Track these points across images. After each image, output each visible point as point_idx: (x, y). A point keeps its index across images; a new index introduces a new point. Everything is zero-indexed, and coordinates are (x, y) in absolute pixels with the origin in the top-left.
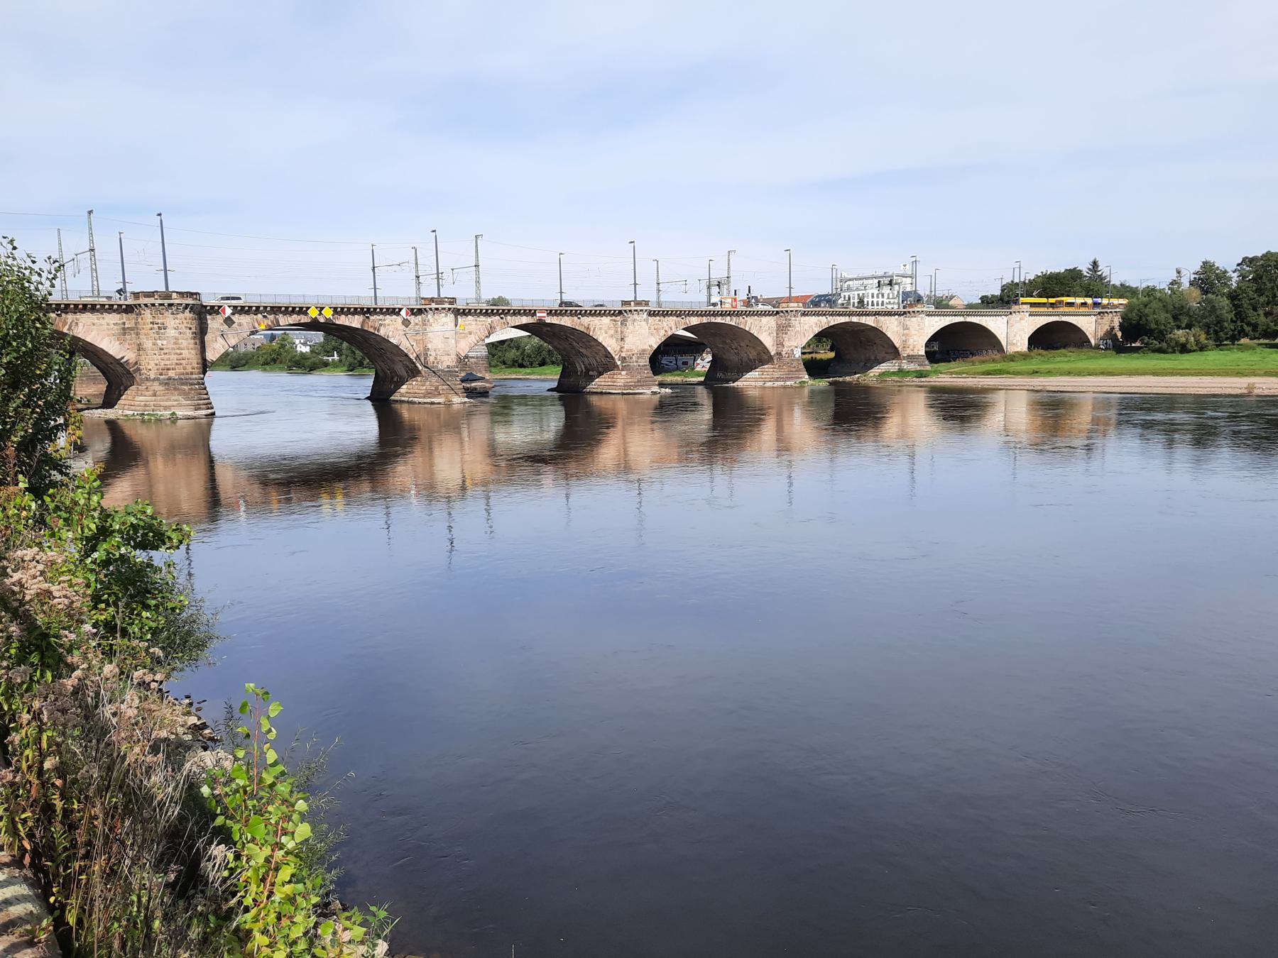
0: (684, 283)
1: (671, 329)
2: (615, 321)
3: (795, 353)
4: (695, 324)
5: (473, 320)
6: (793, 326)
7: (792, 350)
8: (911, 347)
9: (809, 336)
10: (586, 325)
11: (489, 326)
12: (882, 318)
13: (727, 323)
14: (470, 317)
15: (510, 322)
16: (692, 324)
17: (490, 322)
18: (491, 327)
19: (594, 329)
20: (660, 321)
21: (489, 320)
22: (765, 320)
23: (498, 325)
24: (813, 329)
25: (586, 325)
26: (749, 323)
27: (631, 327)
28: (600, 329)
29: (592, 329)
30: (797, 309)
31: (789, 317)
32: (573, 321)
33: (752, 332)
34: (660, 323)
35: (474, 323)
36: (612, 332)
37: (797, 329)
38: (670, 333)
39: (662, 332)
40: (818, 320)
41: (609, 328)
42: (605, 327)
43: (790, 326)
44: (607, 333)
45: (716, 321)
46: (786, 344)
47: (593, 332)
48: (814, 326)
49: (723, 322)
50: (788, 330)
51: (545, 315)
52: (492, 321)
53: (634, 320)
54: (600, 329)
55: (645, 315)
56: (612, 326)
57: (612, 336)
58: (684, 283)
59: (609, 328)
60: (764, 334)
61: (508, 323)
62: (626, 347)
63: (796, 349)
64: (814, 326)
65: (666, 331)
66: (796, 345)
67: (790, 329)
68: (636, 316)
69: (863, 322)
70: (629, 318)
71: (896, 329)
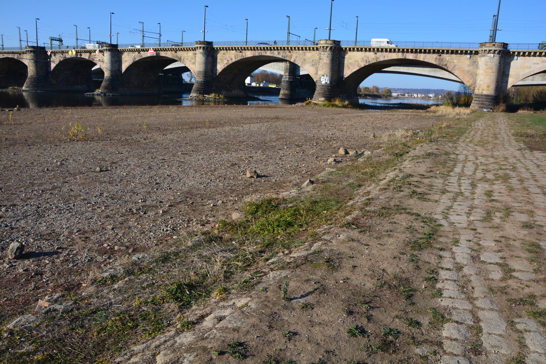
1: (232, 59)
3: (322, 80)
4: (249, 56)
8: (478, 87)
9: (353, 69)
10: (179, 57)
13: (275, 56)
16: (247, 57)
20: (224, 54)
21: (134, 55)
24: (359, 64)
25: (179, 57)
32: (172, 55)
34: (224, 56)
35: (127, 56)
38: (230, 62)
39: (225, 61)
40: (365, 56)
41: (192, 58)
42: (190, 59)
44: (190, 61)
45: (266, 55)
48: (360, 61)
49: (272, 55)
63: (323, 77)
64: (360, 61)
65: (228, 61)
69: (421, 60)
71: (467, 68)
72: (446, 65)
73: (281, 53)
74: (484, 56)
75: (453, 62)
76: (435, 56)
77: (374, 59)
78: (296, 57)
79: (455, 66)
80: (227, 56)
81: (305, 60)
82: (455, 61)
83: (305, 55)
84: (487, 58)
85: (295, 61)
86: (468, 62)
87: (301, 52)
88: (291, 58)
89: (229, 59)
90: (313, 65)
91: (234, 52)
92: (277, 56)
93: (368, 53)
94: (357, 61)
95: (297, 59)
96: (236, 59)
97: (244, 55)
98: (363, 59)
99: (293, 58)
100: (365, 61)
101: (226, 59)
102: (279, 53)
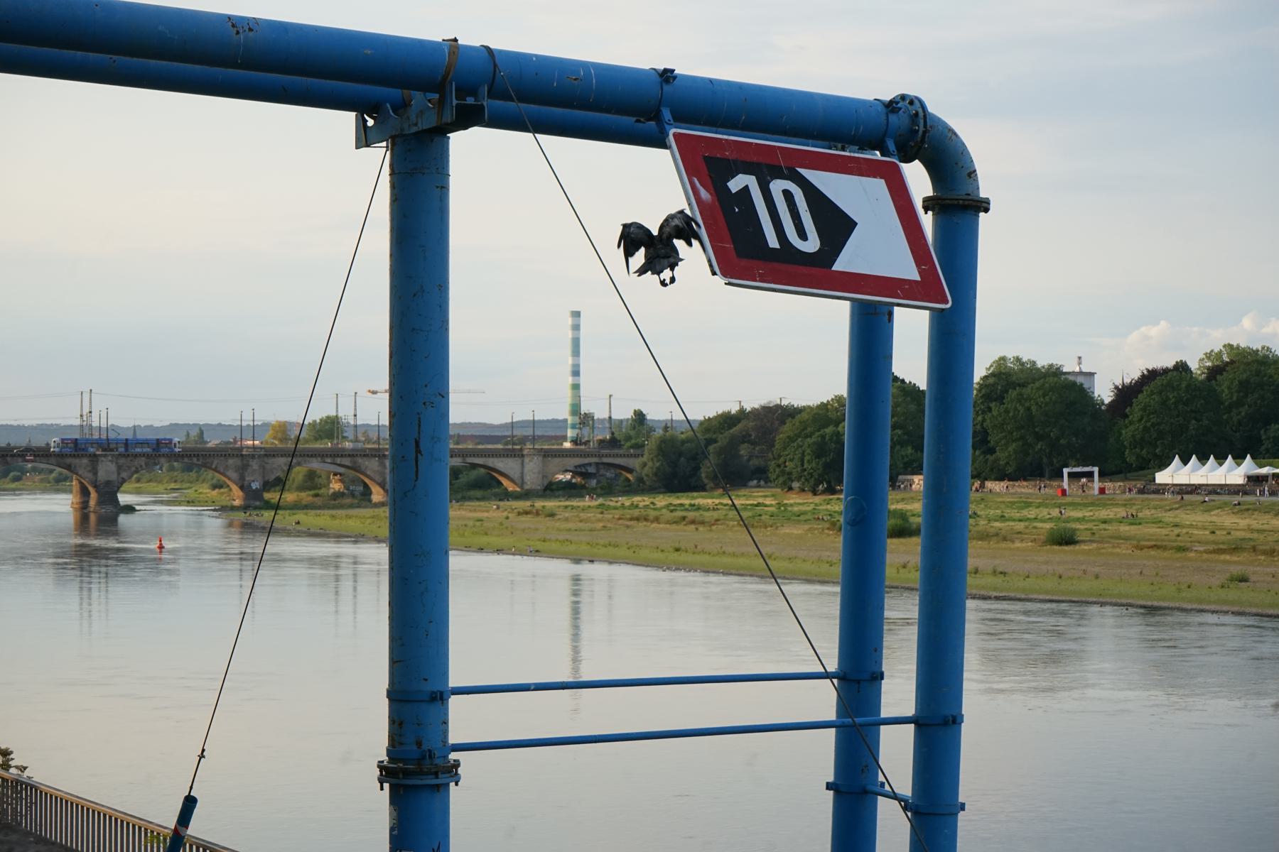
1: (141, 466)
7: (250, 484)
12: (360, 460)
20: (131, 461)
22: (231, 461)
36: (89, 468)
37: (254, 468)
39: (134, 469)
44: (85, 468)
46: (247, 479)
53: (102, 461)
55: (110, 458)
57: (90, 471)
60: (230, 471)
62: (99, 478)
66: (252, 479)
68: (103, 459)
71: (376, 469)
73: (201, 460)
76: (349, 459)
80: (136, 463)
81: (227, 466)
83: (227, 461)
86: (377, 463)
87: (222, 458)
90: (236, 471)
91: (143, 458)
94: (280, 466)
97: (156, 461)
101: (134, 466)
102: (198, 460)
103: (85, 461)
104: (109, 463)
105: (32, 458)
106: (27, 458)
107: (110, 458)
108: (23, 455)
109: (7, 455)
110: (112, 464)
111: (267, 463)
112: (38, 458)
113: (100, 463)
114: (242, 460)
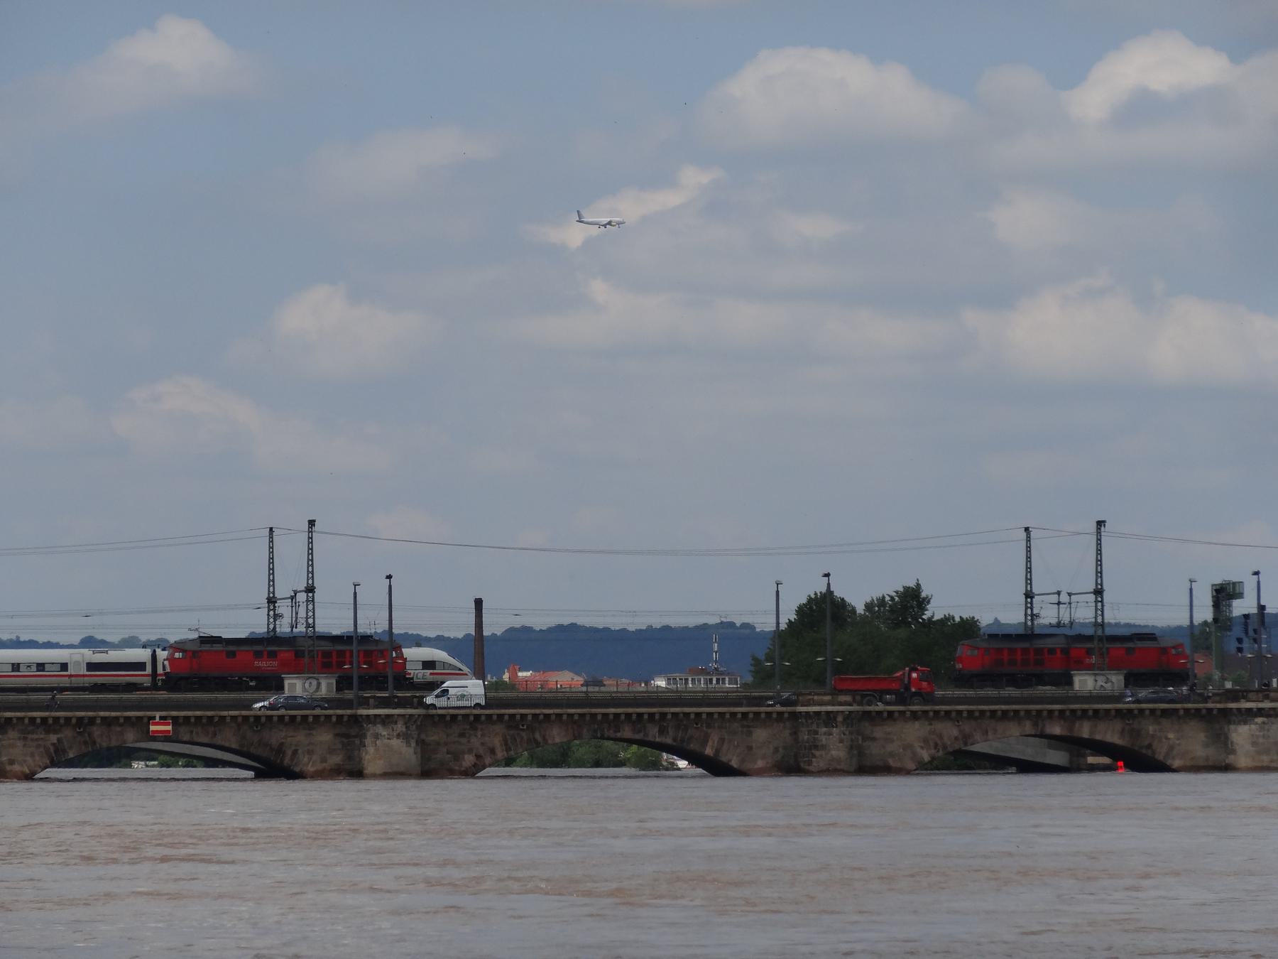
0: (1054, 598)
1: (493, 751)
2: (347, 736)
5: (19, 739)
6: (824, 747)
11: (52, 750)
14: (12, 734)
15: (98, 740)
17: (55, 741)
18: (56, 751)
19: (295, 752)
20: (462, 735)
21: (53, 738)
22: (760, 734)
23: (71, 748)
26: (714, 738)
27: (371, 750)
28: (310, 752)
29: (289, 753)
30: (830, 708)
31: (814, 727)
33: (724, 759)
34: (464, 740)
35: (20, 743)
43: (816, 747)
47: (292, 760)
50: (814, 756)
51: (169, 728)
52: (59, 740)
53: (377, 736)
54: (310, 752)
55: (400, 727)
56: (340, 746)
58: (1054, 598)
59: (332, 751)
61: (94, 743)
65: (478, 757)
67: (817, 753)
68: (380, 729)
70: (368, 730)
72: (1149, 746)
73: (671, 732)
74: (1245, 723)
75: (1167, 738)
76: (1118, 725)
77: (956, 738)
78: (722, 740)
79: (1171, 748)
80: (475, 742)
81: (750, 748)
82: (1171, 736)
83: (750, 734)
84: (1253, 726)
85: (717, 751)
88: (704, 743)
89: (481, 752)
91: (499, 728)
92: (658, 740)
93: (939, 726)
95: (725, 747)
96: (508, 749)
97: (538, 736)
98: (926, 741)
99: (710, 743)
100: (932, 744)
101: (470, 751)
102: (662, 731)
103: (324, 737)
104: (396, 742)
105: (169, 728)
106: (152, 728)
107: (400, 727)
108: (139, 718)
109: (92, 721)
110: (408, 744)
111: (874, 739)
112: (183, 729)
113: (368, 741)
114: (795, 733)
